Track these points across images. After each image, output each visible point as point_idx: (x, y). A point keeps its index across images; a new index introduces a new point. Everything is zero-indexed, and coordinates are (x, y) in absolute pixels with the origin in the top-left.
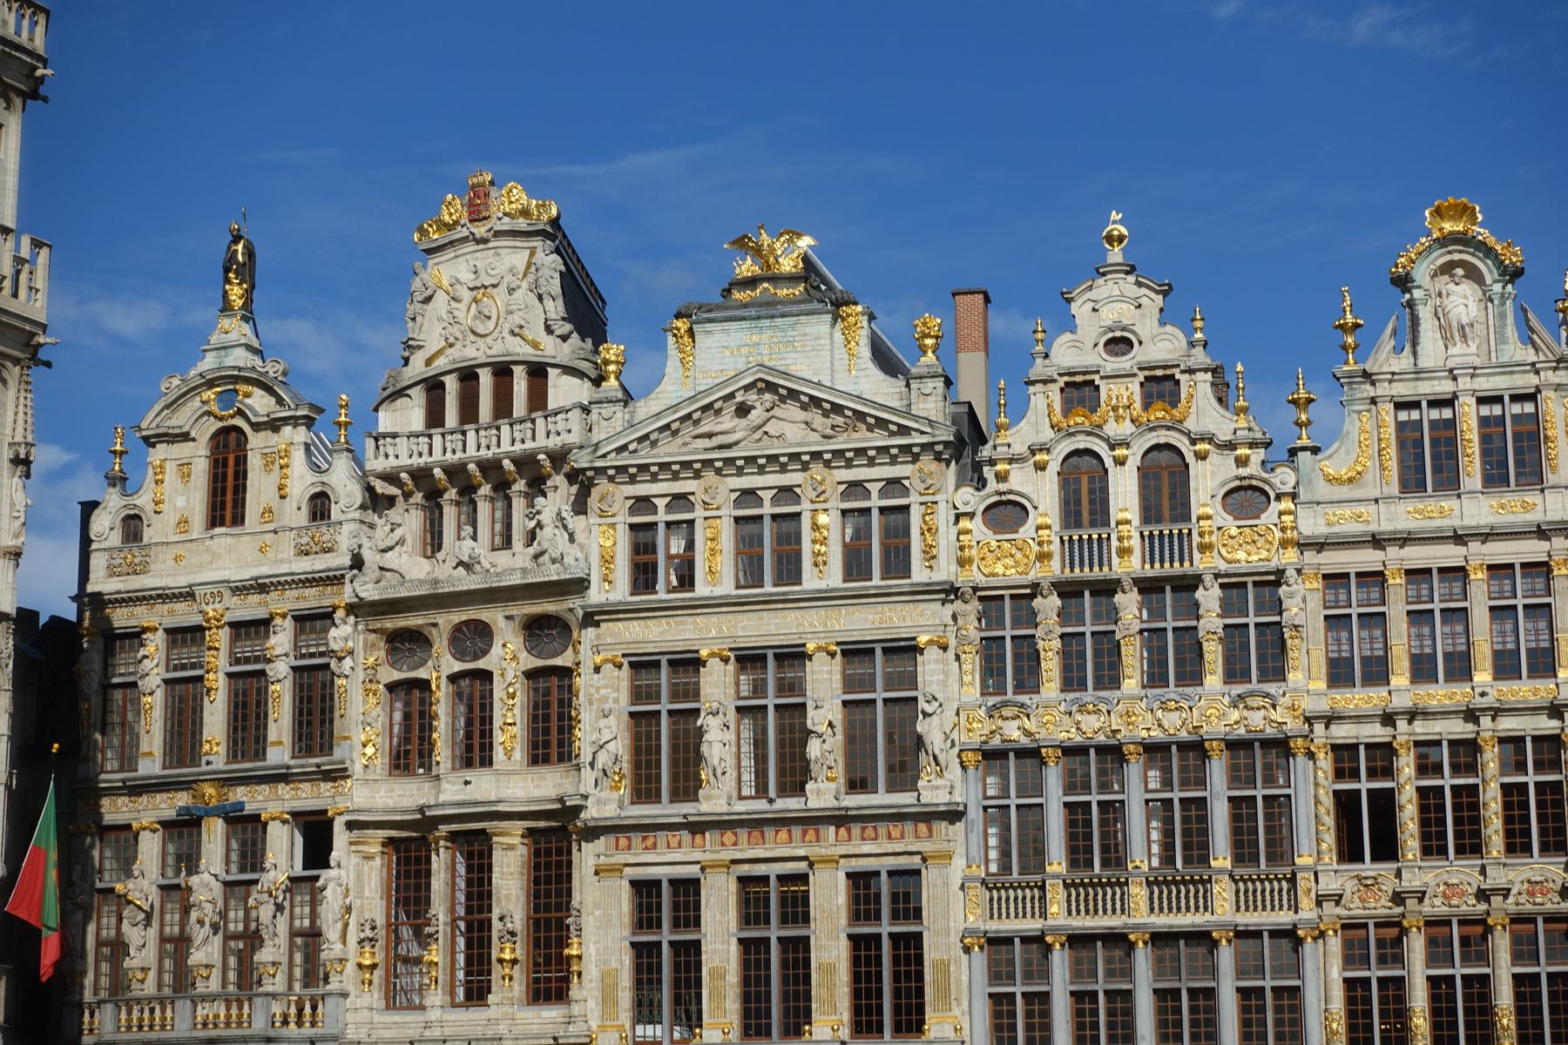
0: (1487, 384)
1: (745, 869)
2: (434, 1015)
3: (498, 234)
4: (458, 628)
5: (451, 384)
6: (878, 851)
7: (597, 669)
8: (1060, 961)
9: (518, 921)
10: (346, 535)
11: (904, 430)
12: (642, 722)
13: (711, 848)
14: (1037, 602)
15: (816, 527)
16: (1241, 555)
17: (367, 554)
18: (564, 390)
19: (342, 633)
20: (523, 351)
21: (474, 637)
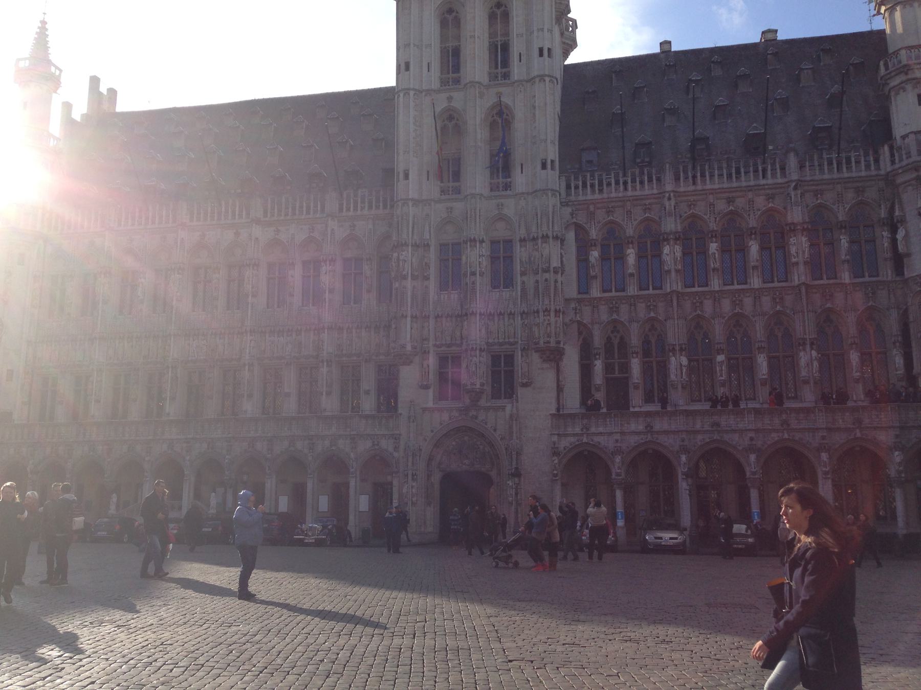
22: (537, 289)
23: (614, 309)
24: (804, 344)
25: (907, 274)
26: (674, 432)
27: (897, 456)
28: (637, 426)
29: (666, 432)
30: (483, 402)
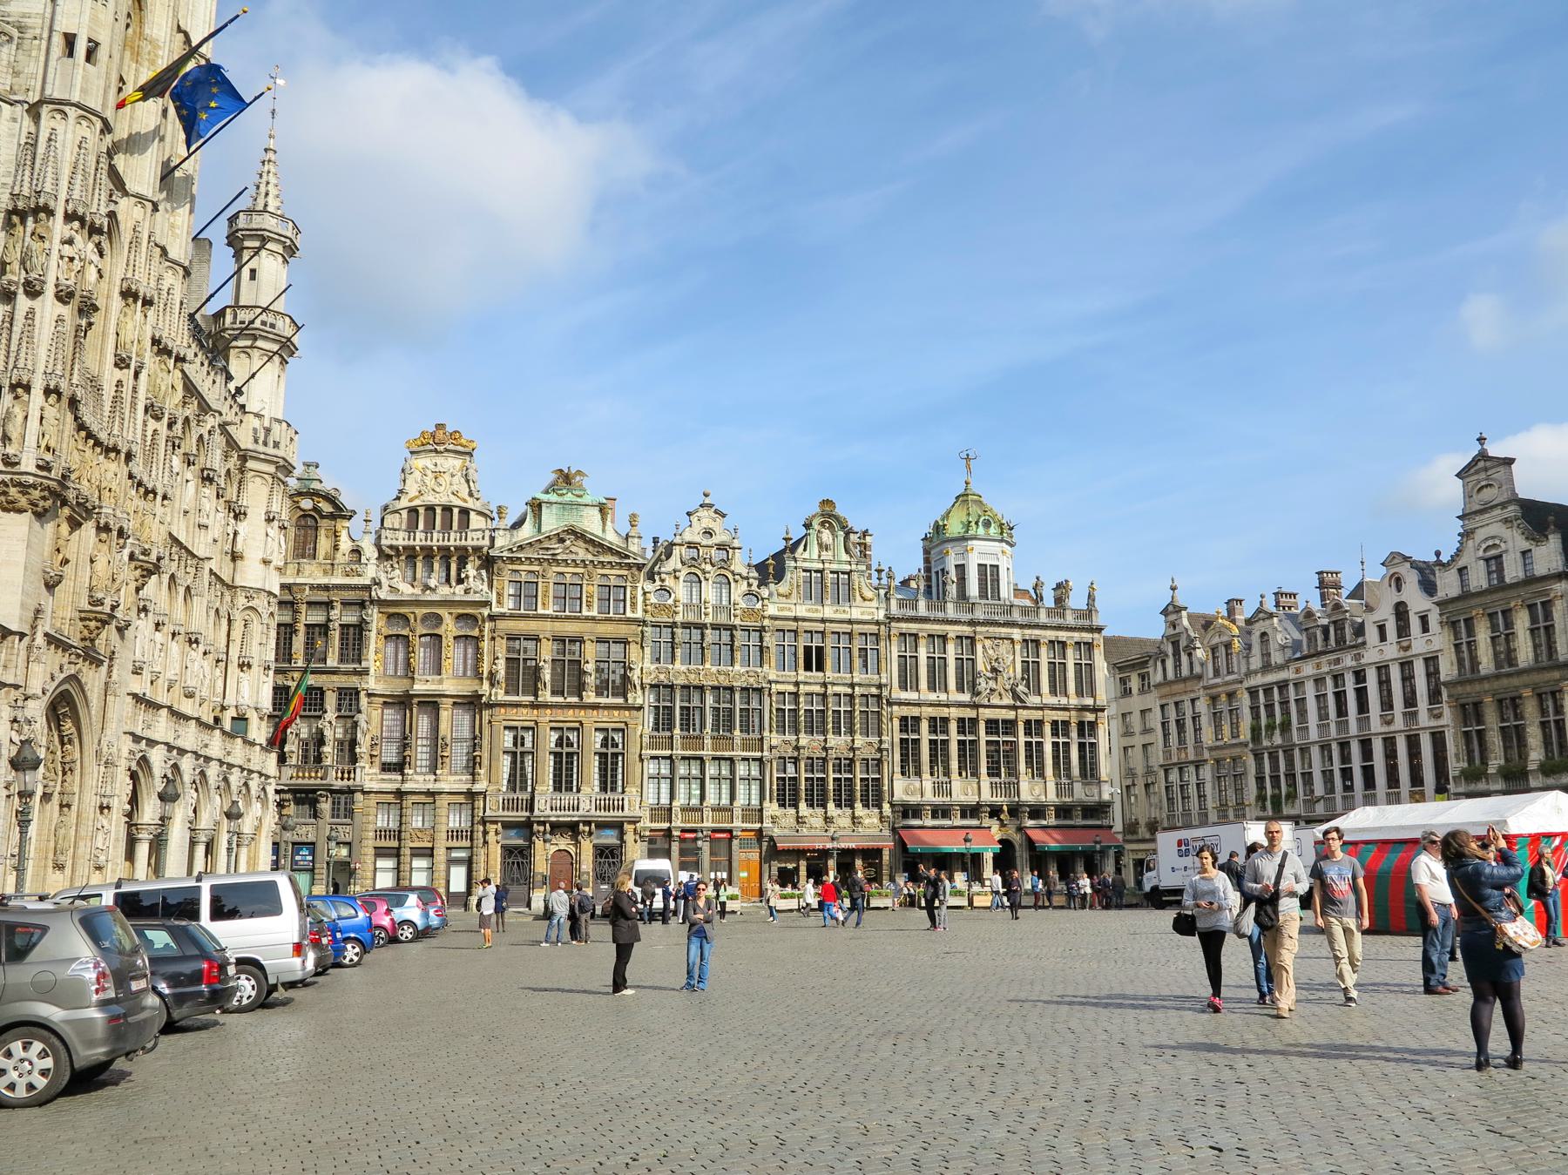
0: (835, 567)
3: (447, 450)
5: (422, 510)
7: (493, 639)
10: (371, 571)
11: (627, 557)
17: (384, 580)
18: (476, 521)
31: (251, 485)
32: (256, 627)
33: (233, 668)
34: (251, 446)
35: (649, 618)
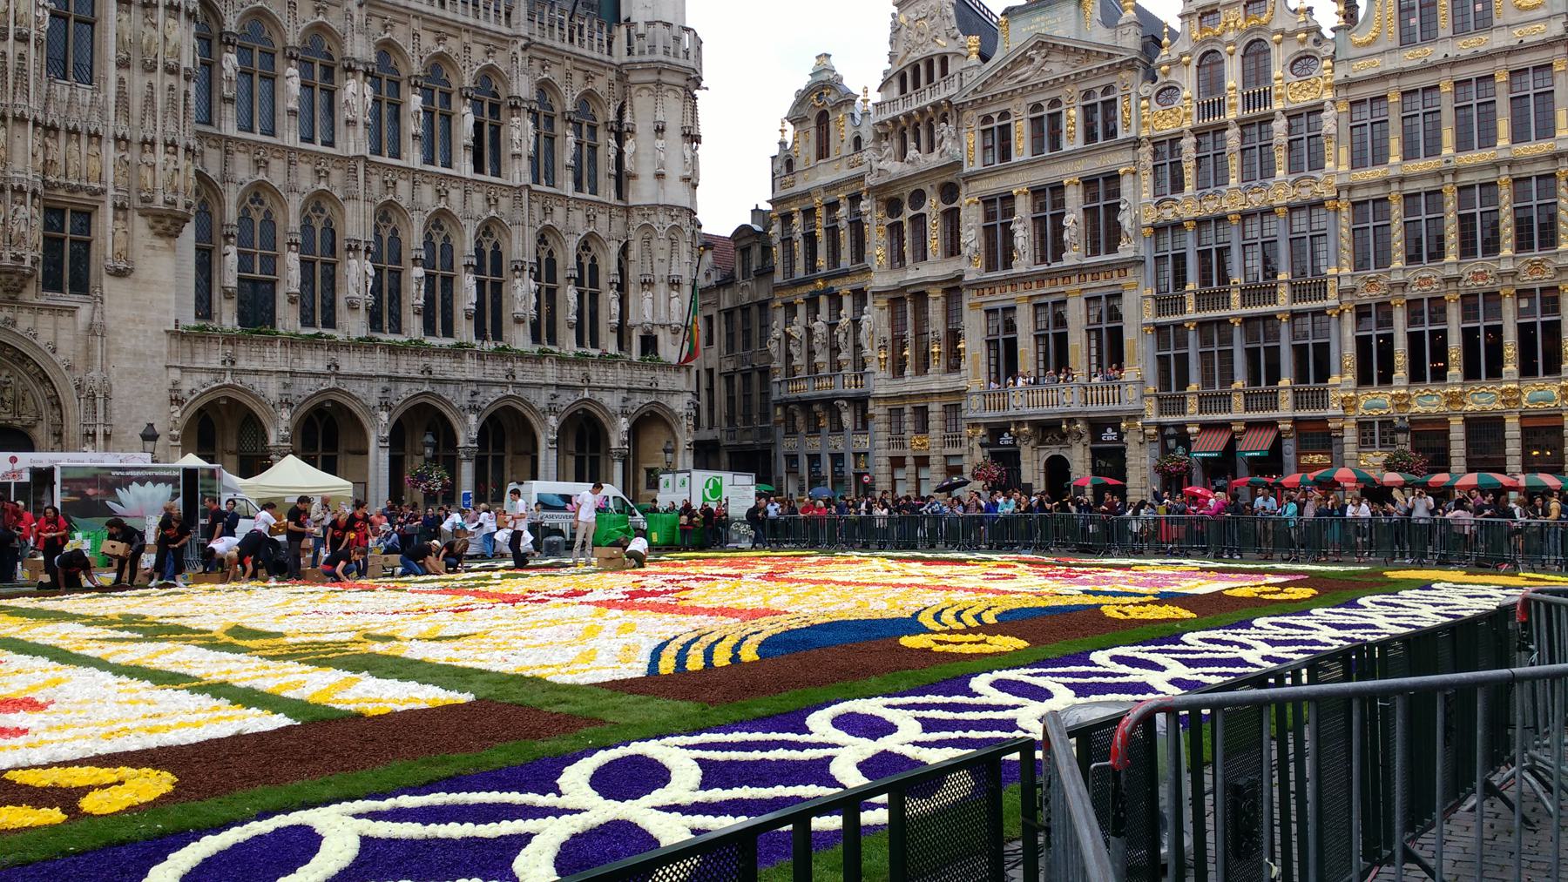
1: (1037, 300)
2: (907, 380)
4: (912, 195)
6: (1101, 285)
8: (1192, 337)
9: (942, 333)
10: (868, 154)
11: (1110, 56)
12: (989, 231)
13: (1022, 293)
14: (1183, 142)
15: (1069, 118)
16: (1301, 99)
19: (865, 205)
20: (939, 50)
21: (918, 198)
22: (150, 99)
23: (262, 165)
24: (523, 269)
25: (633, 200)
26: (370, 378)
27: (624, 424)
28: (408, 366)
29: (359, 377)
30: (30, 295)
31: (637, 101)
32: (660, 246)
33: (632, 288)
34: (625, 59)
35: (1144, 133)
